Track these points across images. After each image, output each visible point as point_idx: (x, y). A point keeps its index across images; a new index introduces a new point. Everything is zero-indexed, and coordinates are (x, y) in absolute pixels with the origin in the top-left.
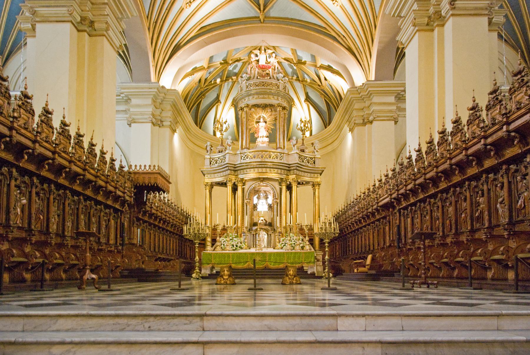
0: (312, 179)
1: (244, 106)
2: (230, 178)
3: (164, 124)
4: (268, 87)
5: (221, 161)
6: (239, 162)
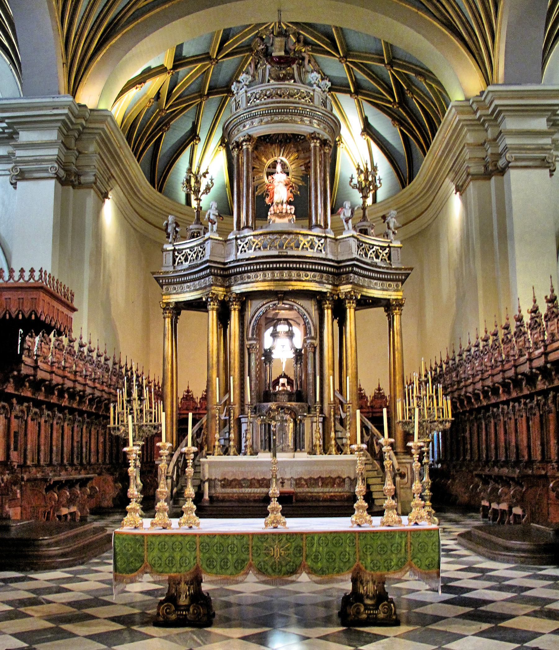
0: (385, 293)
1: (242, 139)
2: (213, 294)
3: (82, 181)
4: (291, 99)
5: (195, 256)
6: (232, 258)
